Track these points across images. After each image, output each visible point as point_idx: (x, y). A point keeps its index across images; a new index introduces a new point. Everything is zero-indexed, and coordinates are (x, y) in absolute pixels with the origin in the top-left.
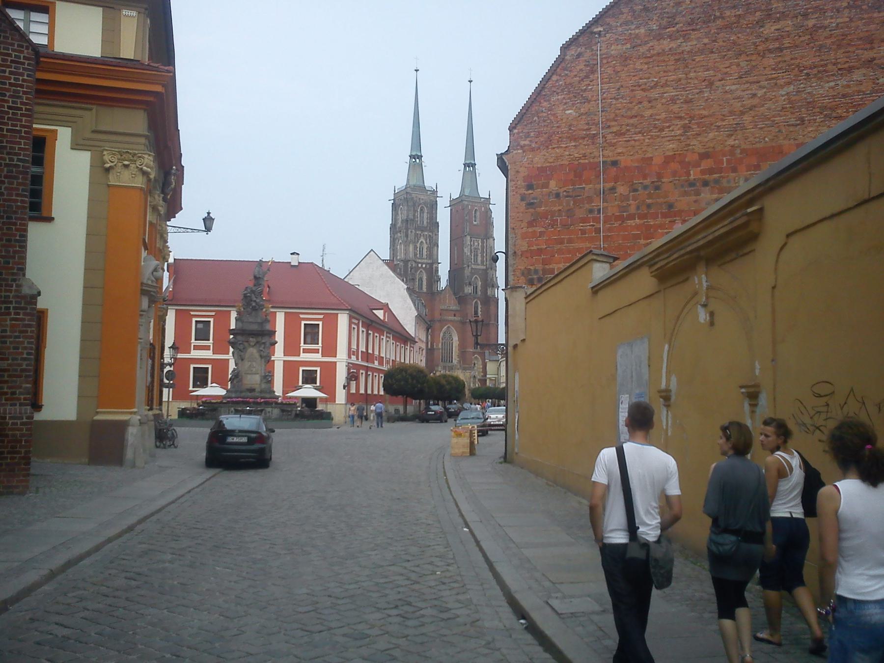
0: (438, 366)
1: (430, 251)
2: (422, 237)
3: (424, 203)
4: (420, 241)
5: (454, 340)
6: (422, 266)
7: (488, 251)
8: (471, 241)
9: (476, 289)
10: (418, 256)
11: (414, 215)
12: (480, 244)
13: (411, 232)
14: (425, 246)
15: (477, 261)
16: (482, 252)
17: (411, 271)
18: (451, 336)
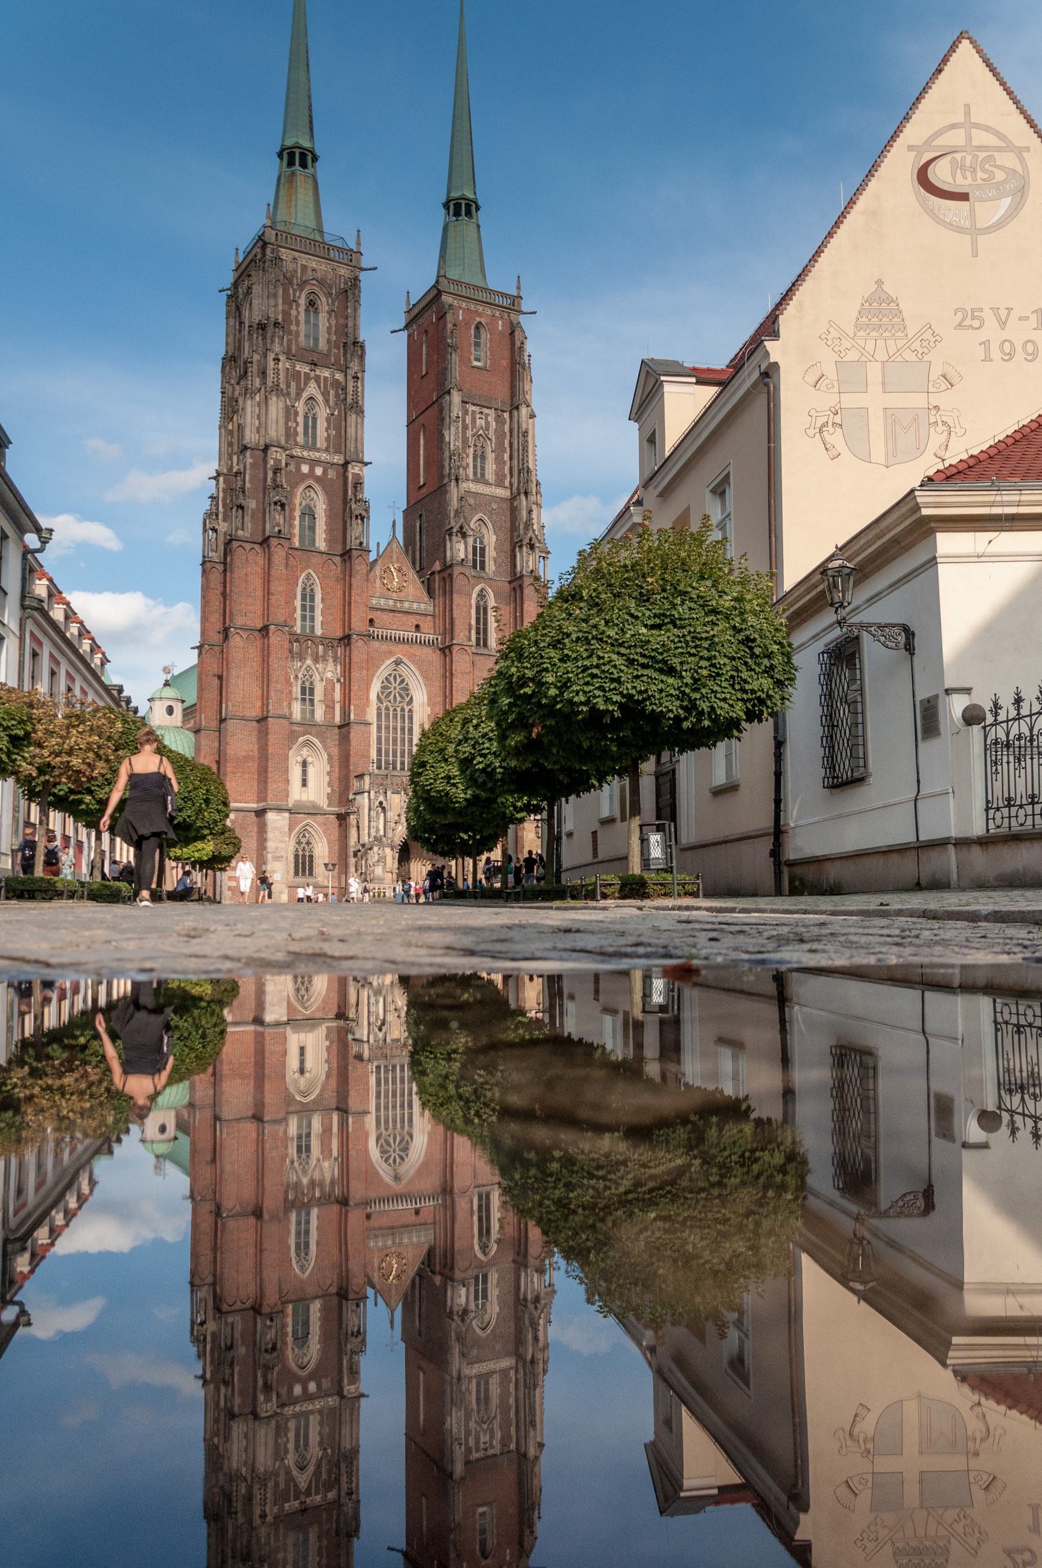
0: (360, 777)
1: (338, 429)
2: (312, 384)
3: (321, 282)
4: (305, 395)
5: (414, 703)
6: (312, 470)
7: (515, 446)
8: (466, 412)
9: (483, 555)
10: (300, 439)
11: (286, 314)
12: (493, 425)
13: (277, 360)
14: (322, 413)
15: (483, 475)
16: (499, 450)
17: (274, 480)
18: (406, 689)
